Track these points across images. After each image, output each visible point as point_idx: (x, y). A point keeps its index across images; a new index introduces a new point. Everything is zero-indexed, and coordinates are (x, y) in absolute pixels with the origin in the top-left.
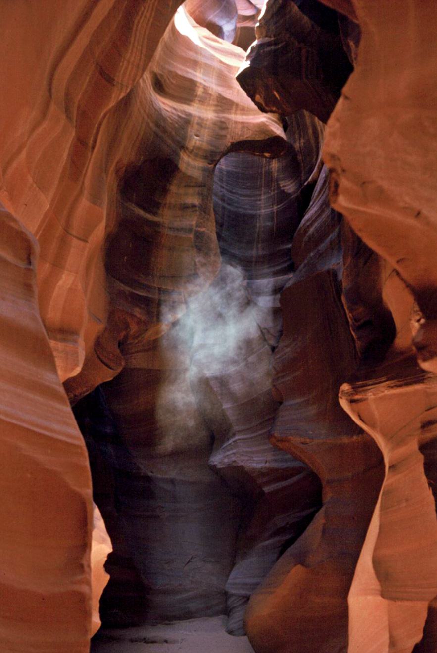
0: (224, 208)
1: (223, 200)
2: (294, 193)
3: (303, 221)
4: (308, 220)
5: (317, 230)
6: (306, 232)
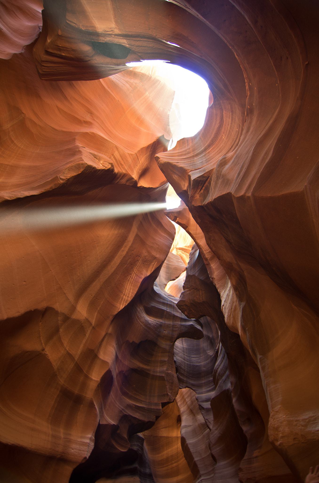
0: (185, 363)
1: (184, 359)
2: (212, 355)
3: (215, 367)
4: (217, 365)
5: (221, 370)
6: (217, 371)
